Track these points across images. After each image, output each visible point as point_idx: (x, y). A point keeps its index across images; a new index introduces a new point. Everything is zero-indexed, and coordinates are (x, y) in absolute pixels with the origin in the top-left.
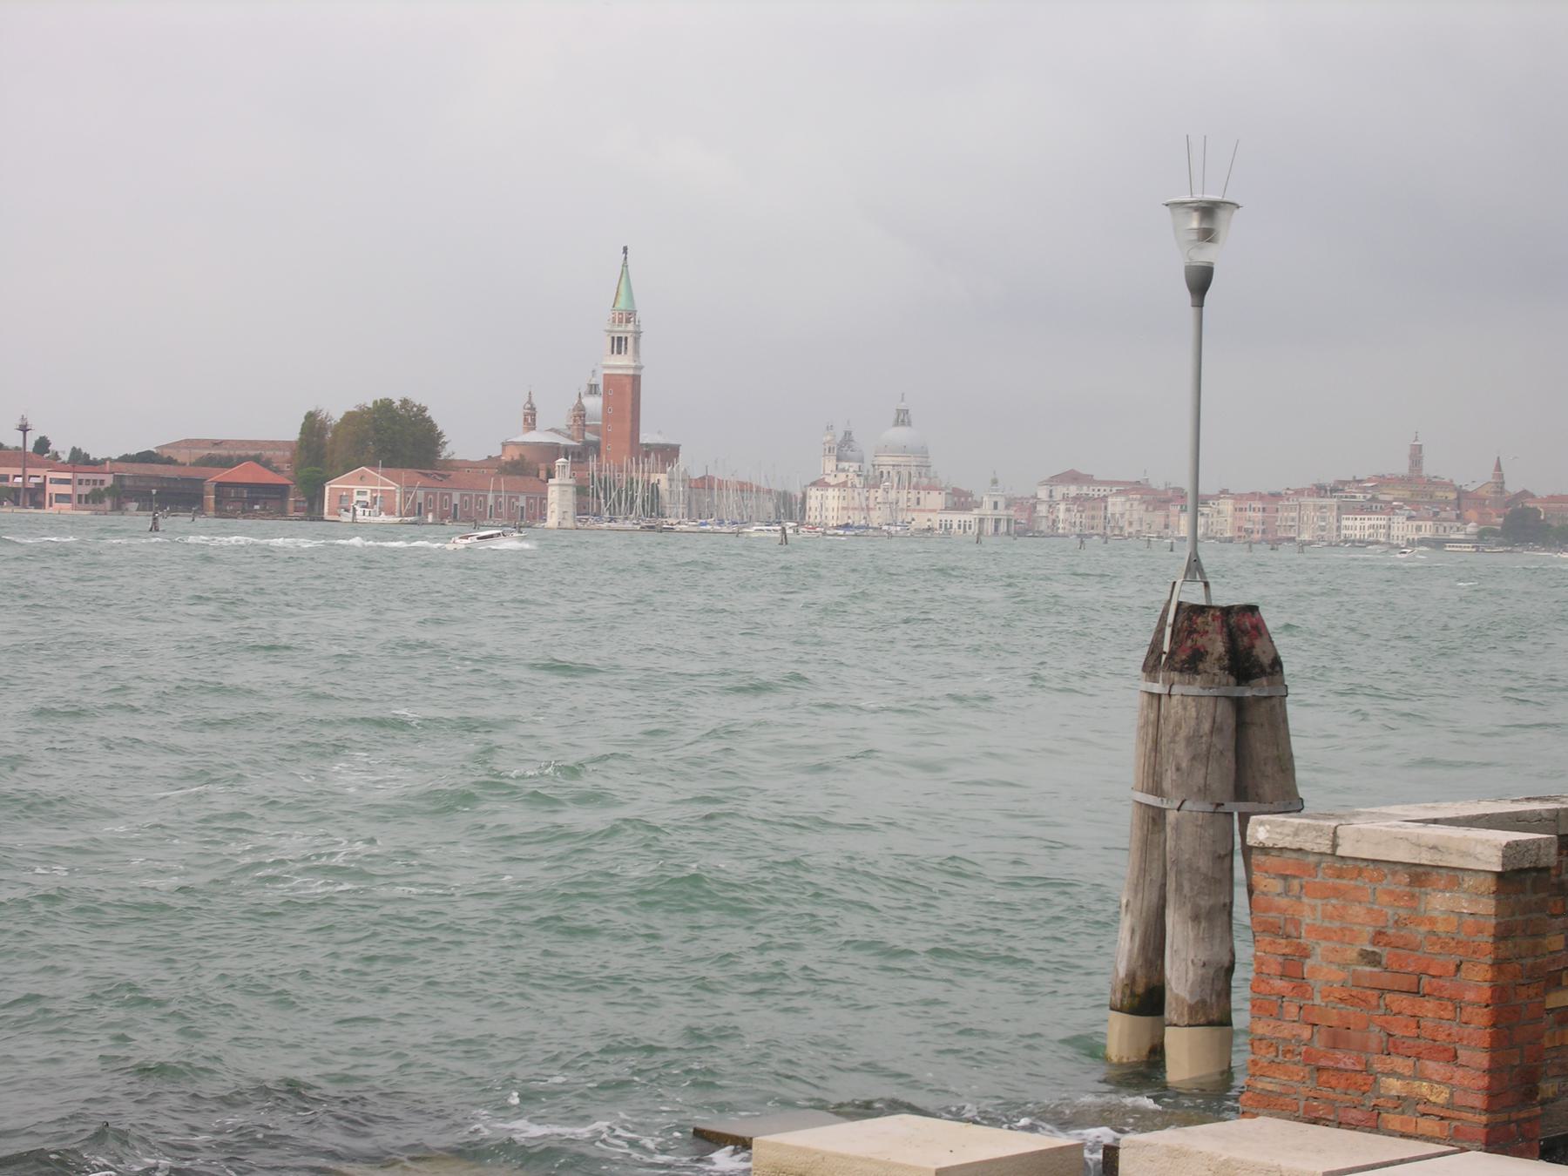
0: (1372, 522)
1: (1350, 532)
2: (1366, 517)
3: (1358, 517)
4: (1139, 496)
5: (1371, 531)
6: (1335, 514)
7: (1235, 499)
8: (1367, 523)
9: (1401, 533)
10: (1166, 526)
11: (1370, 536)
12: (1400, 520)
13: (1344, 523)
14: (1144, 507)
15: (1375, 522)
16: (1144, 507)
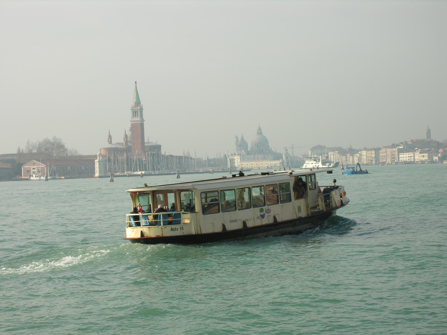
0: (409, 155)
1: (402, 159)
2: (407, 153)
3: (405, 154)
4: (338, 152)
5: (409, 158)
6: (397, 153)
7: (366, 151)
8: (407, 155)
9: (418, 158)
10: (346, 161)
11: (408, 159)
12: (417, 154)
13: (400, 156)
14: (339, 155)
15: (410, 155)
16: (339, 155)
